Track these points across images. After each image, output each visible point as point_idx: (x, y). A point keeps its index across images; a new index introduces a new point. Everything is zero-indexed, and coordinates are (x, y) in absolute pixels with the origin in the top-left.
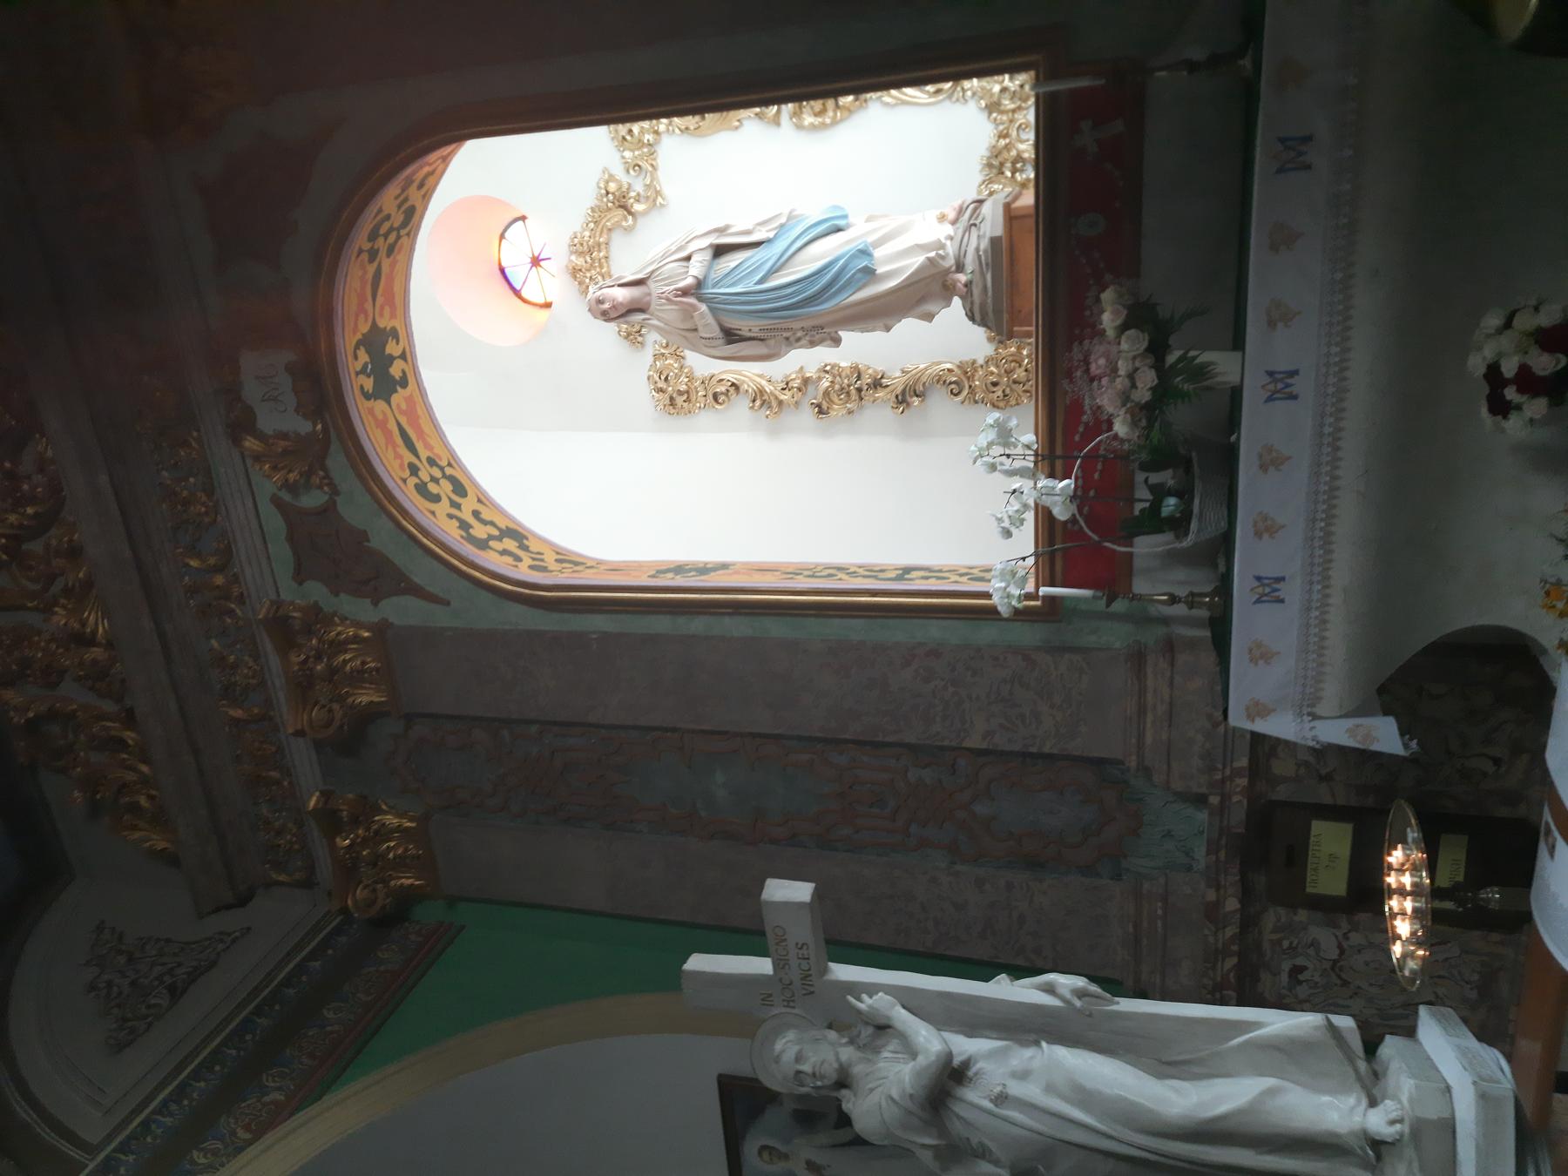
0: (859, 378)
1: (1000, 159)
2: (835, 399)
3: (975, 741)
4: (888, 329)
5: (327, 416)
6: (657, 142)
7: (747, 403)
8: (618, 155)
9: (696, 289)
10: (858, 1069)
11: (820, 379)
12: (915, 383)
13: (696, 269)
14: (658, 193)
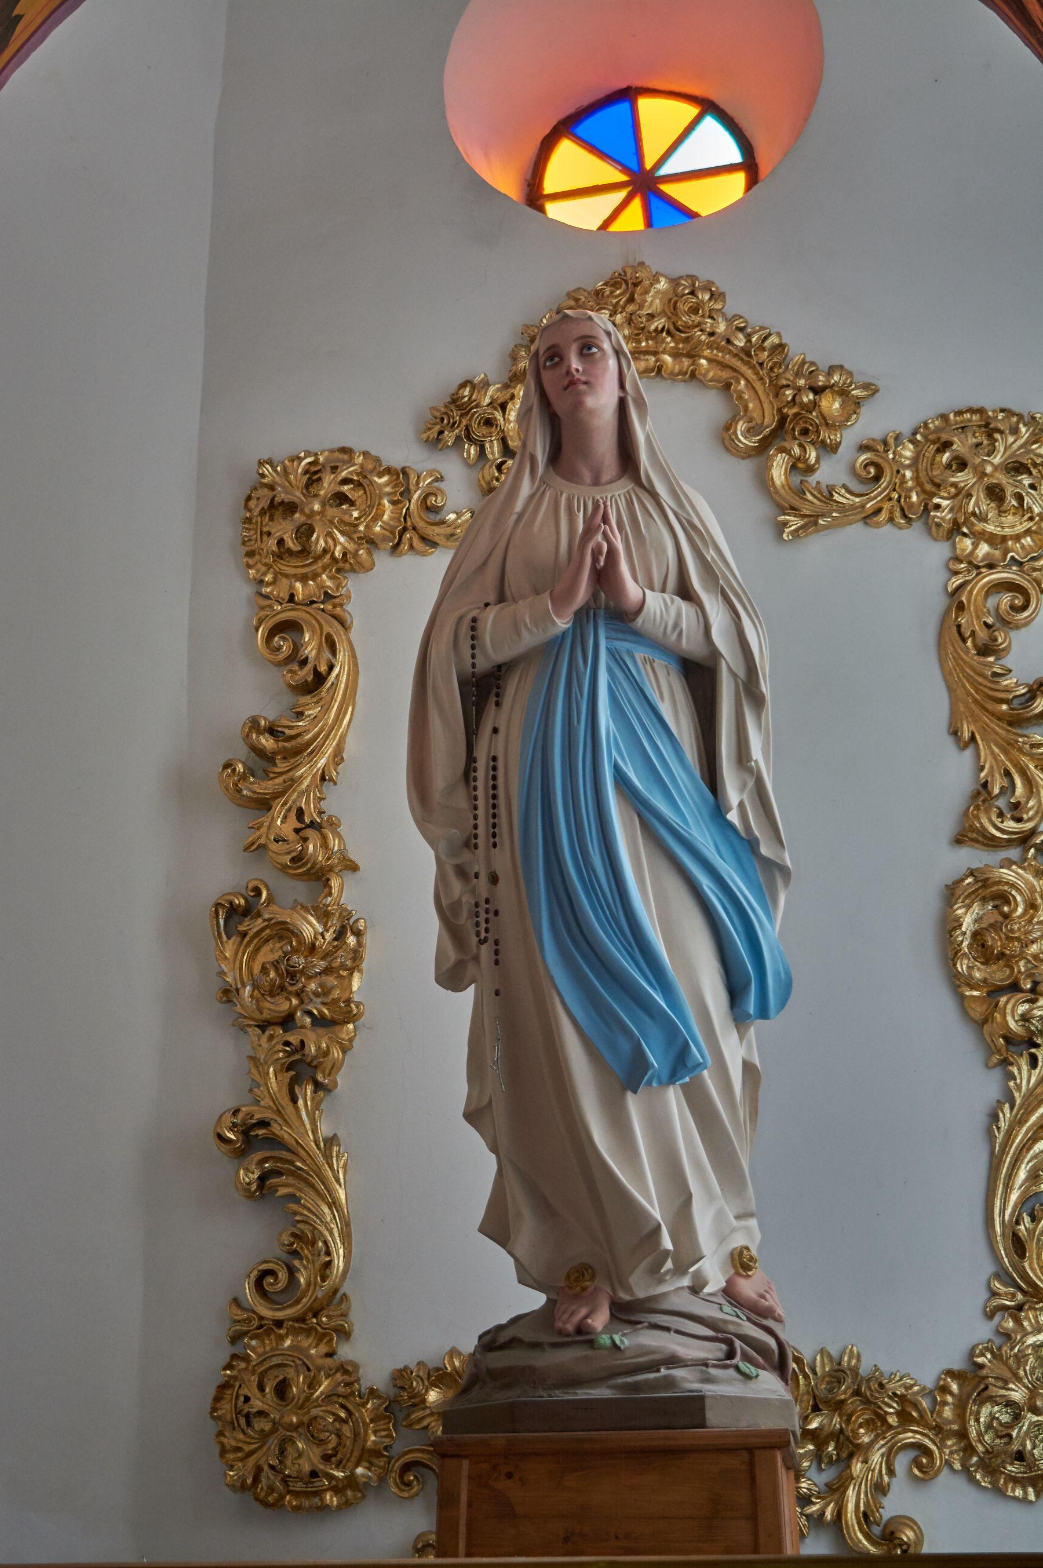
0: (320, 1022)
1: (853, 1403)
2: (269, 954)
4: (473, 1116)
6: (932, 529)
7: (269, 712)
8: (906, 429)
11: (324, 916)
12: (296, 1173)
13: (659, 607)
14: (811, 522)
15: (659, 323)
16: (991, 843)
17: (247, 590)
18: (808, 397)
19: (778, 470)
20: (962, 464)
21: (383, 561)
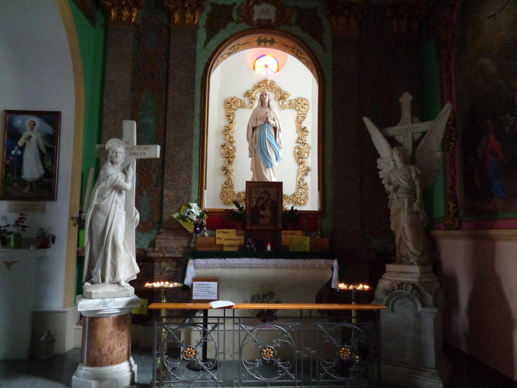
0: (232, 158)
3: (165, 192)
4: (251, 170)
5: (257, 27)
9: (267, 122)
10: (116, 166)
13: (272, 122)
14: (284, 108)
16: (299, 143)
17: (224, 111)
19: (281, 102)
21: (239, 109)
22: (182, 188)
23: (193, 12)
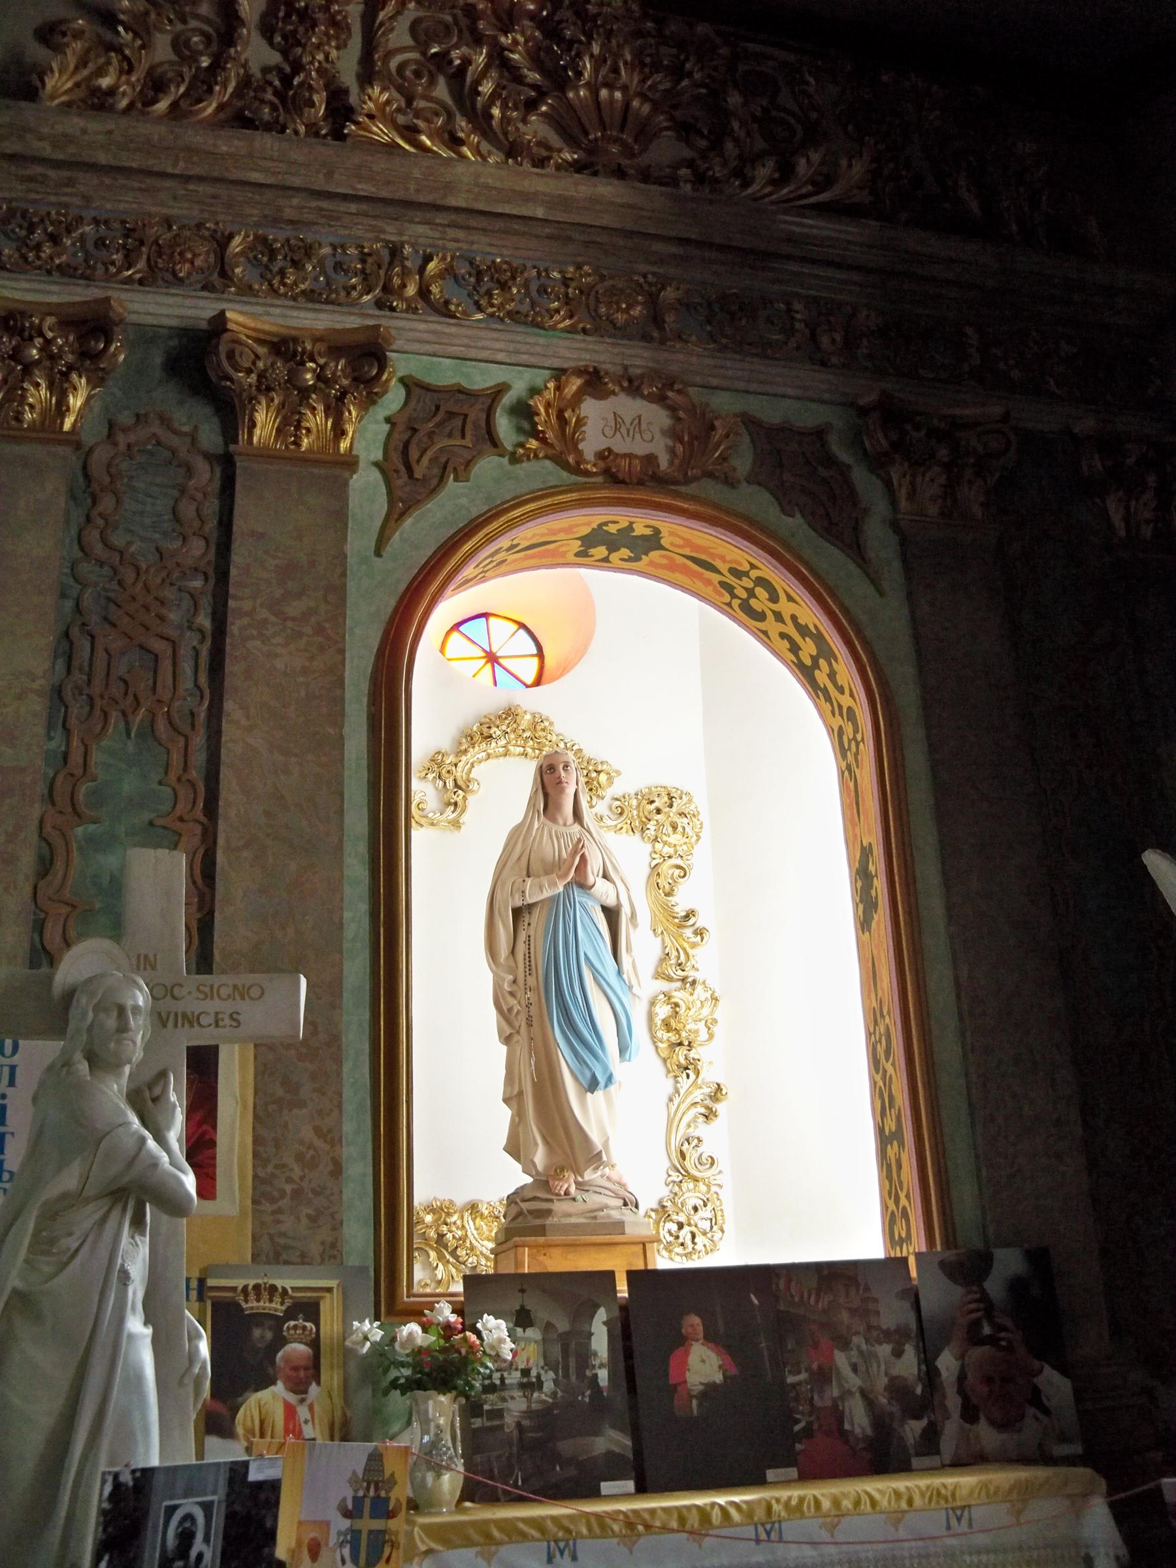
4: (506, 1100)
5: (600, 479)
8: (633, 792)
15: (527, 734)
16: (670, 979)
18: (594, 775)
20: (658, 811)
22: (297, 1193)
23: (335, 410)
